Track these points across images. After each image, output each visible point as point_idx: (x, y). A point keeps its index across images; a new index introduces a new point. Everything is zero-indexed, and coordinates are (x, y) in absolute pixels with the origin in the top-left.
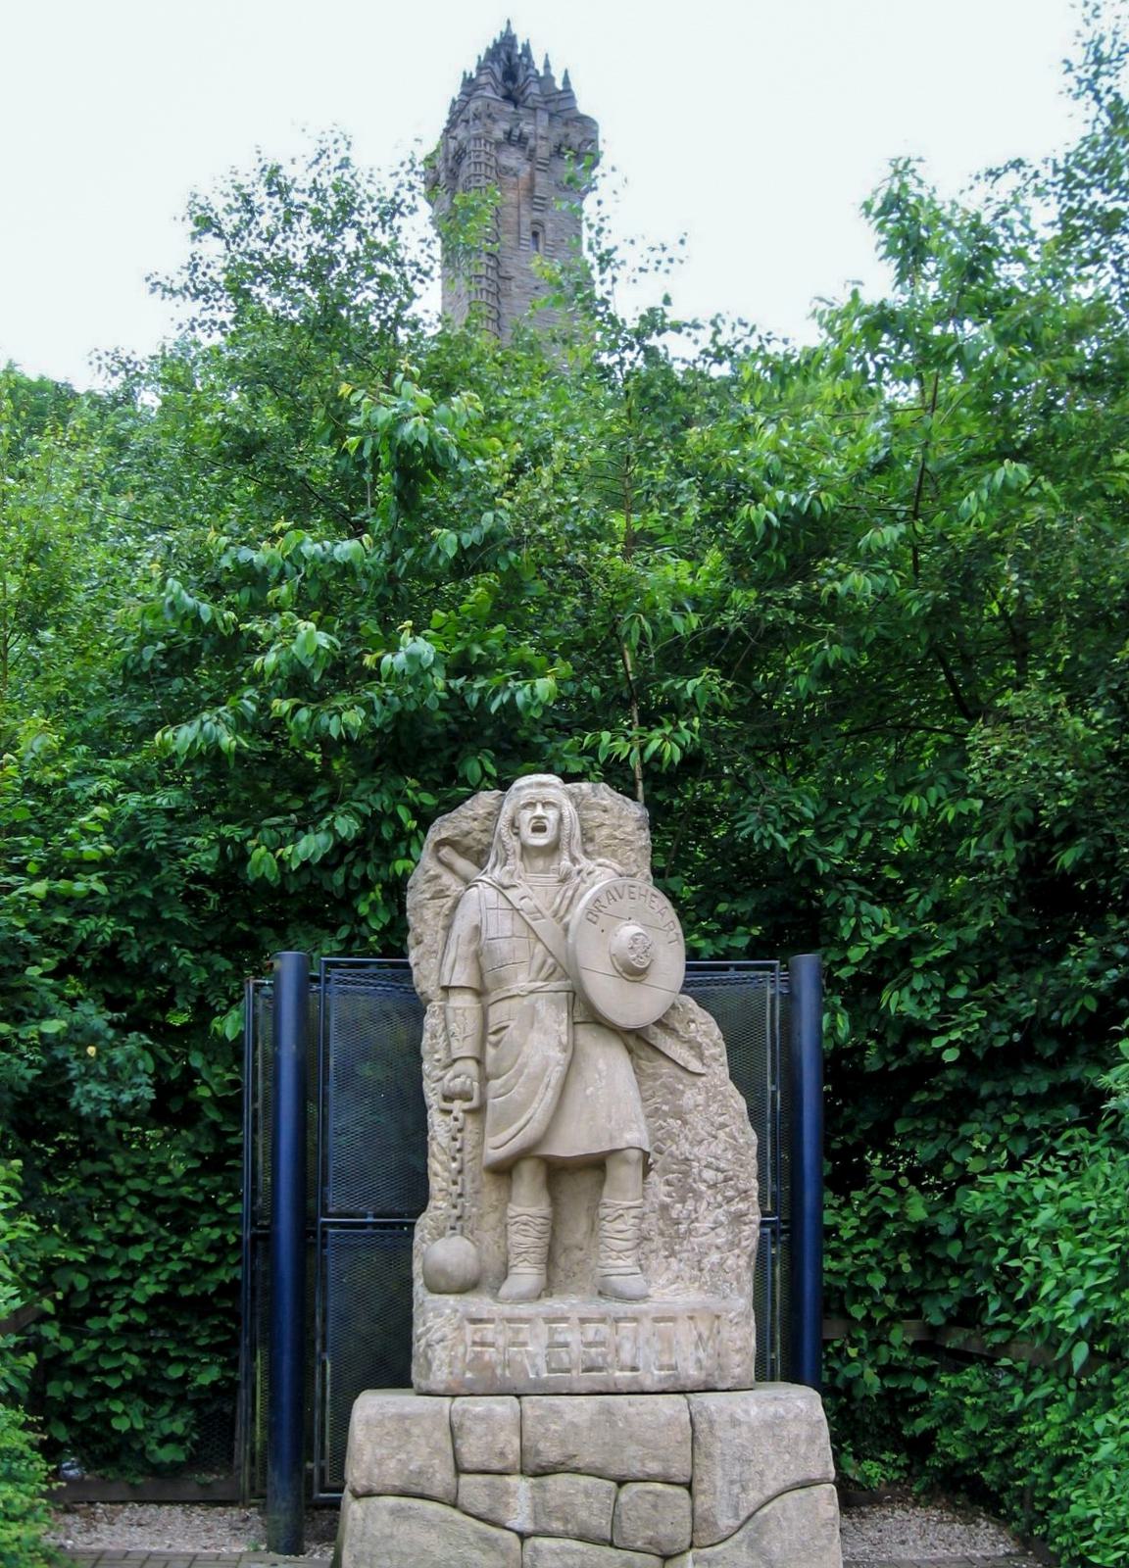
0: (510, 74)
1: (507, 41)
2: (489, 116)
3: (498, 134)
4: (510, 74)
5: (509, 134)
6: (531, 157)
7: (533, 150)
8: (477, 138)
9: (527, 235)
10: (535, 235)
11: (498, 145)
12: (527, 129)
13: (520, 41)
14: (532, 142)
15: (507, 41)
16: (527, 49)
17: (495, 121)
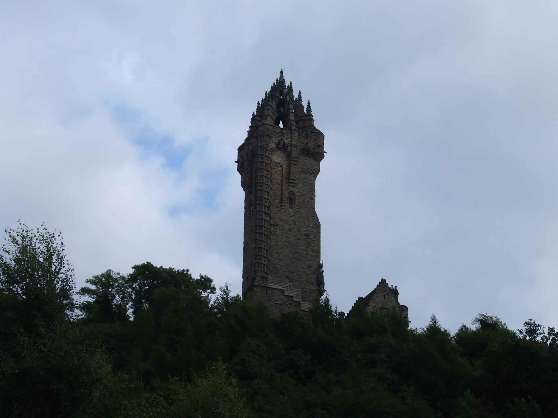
0: (281, 104)
1: (280, 82)
2: (268, 135)
3: (273, 145)
4: (281, 104)
5: (278, 145)
6: (289, 156)
7: (290, 153)
8: (262, 147)
9: (286, 201)
10: (291, 199)
11: (272, 150)
12: (287, 141)
13: (287, 84)
14: (289, 148)
15: (280, 82)
16: (290, 88)
17: (271, 138)
